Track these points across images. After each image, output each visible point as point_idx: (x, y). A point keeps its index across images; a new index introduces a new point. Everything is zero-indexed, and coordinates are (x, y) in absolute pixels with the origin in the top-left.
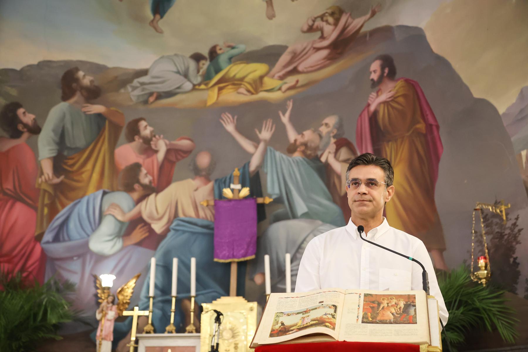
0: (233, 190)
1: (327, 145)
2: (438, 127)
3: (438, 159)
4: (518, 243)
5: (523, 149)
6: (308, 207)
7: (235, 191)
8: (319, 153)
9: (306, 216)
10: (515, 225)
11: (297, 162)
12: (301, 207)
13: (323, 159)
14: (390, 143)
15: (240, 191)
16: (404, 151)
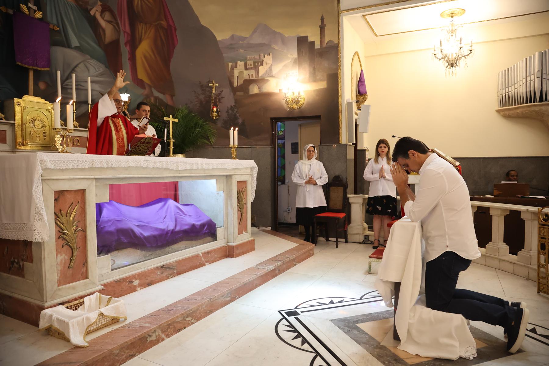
0: (29, 8)
1: (95, 4)
2: (175, 29)
3: (174, 47)
4: (220, 102)
5: (230, 62)
6: (79, 43)
7: (32, 11)
8: (89, 7)
9: (77, 48)
10: (219, 94)
11: (71, 6)
12: (75, 42)
13: (92, 13)
14: (142, 24)
15: (35, 11)
16: (151, 33)
